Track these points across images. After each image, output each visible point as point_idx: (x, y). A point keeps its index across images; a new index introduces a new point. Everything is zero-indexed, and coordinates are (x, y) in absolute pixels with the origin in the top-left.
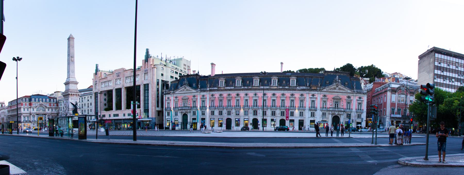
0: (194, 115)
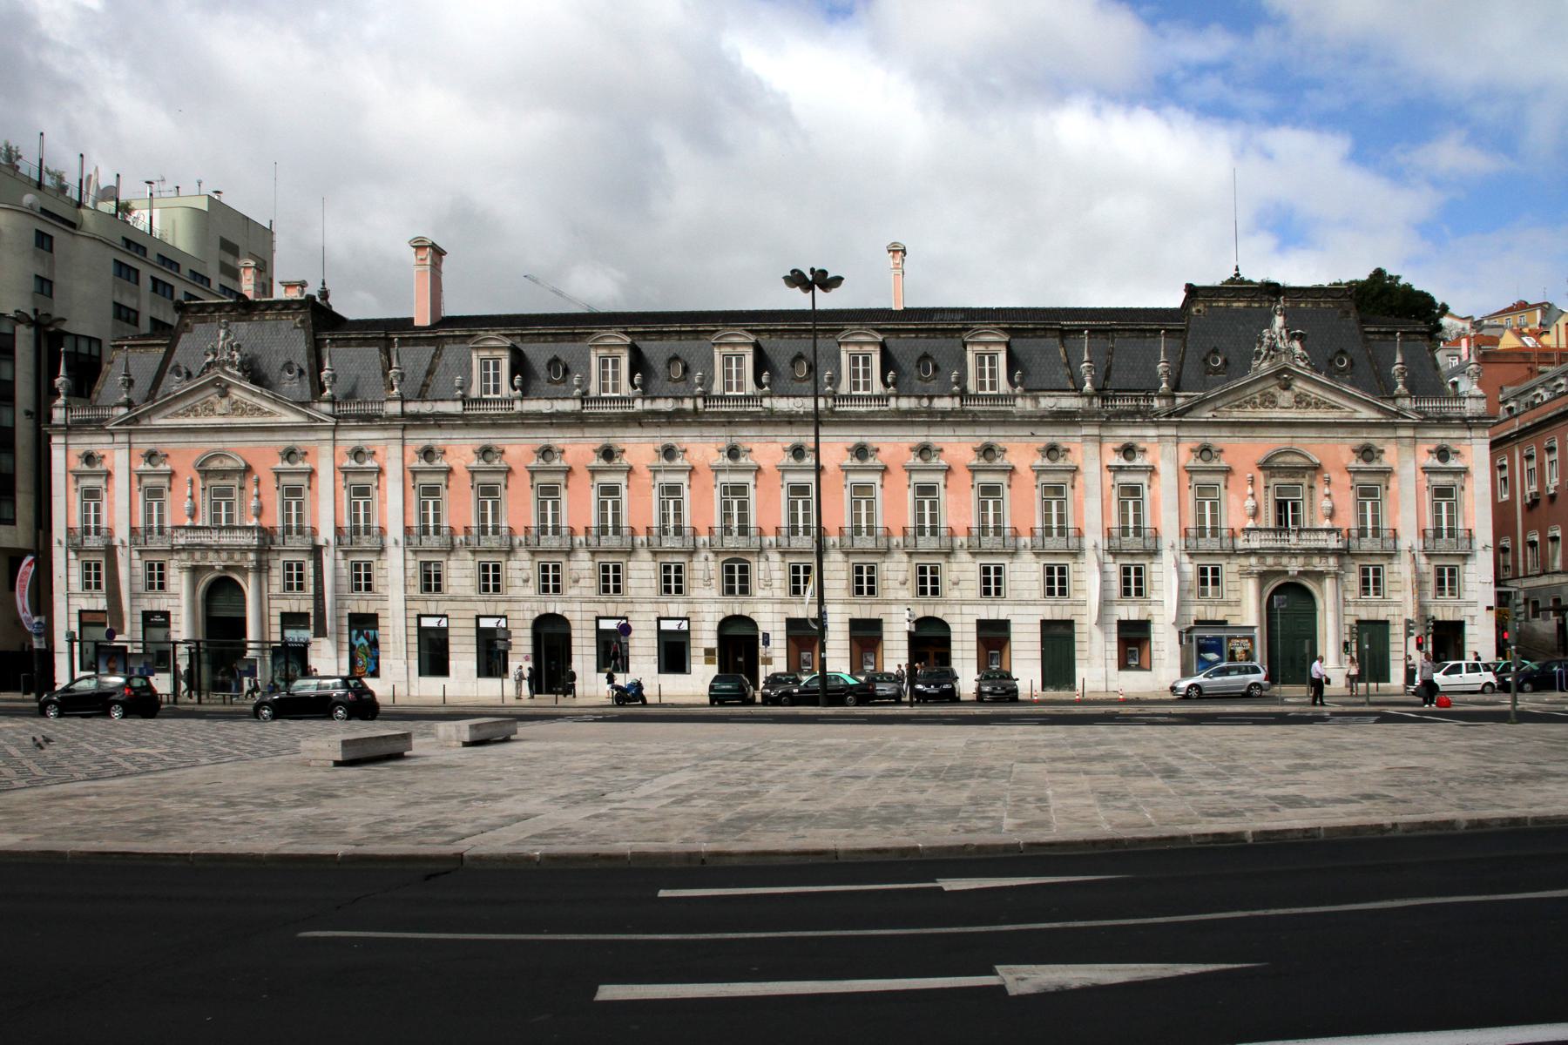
0: (290, 587)
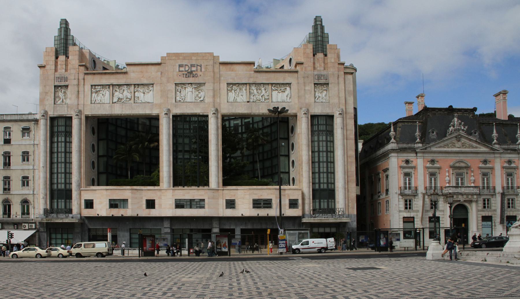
0: (484, 207)
